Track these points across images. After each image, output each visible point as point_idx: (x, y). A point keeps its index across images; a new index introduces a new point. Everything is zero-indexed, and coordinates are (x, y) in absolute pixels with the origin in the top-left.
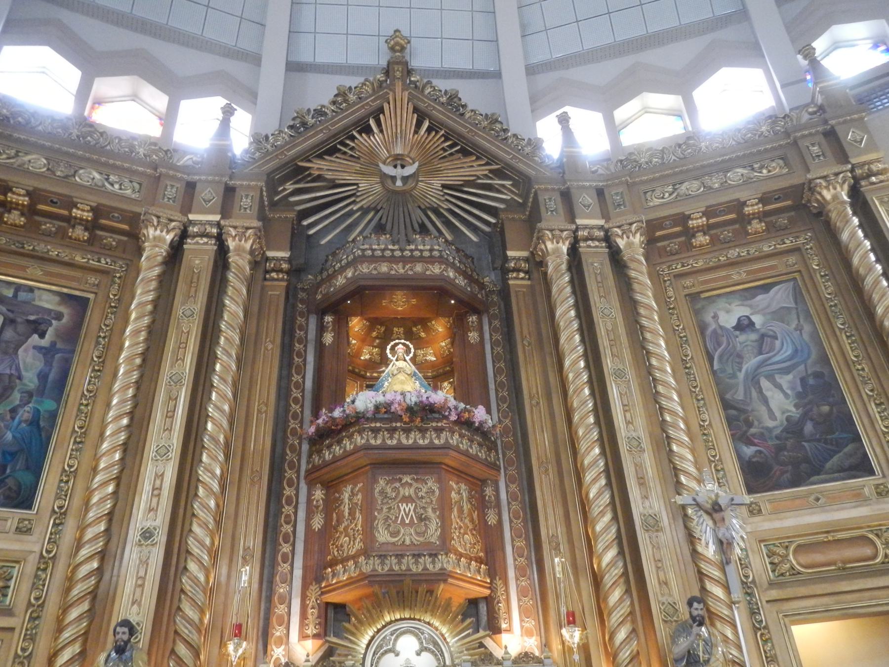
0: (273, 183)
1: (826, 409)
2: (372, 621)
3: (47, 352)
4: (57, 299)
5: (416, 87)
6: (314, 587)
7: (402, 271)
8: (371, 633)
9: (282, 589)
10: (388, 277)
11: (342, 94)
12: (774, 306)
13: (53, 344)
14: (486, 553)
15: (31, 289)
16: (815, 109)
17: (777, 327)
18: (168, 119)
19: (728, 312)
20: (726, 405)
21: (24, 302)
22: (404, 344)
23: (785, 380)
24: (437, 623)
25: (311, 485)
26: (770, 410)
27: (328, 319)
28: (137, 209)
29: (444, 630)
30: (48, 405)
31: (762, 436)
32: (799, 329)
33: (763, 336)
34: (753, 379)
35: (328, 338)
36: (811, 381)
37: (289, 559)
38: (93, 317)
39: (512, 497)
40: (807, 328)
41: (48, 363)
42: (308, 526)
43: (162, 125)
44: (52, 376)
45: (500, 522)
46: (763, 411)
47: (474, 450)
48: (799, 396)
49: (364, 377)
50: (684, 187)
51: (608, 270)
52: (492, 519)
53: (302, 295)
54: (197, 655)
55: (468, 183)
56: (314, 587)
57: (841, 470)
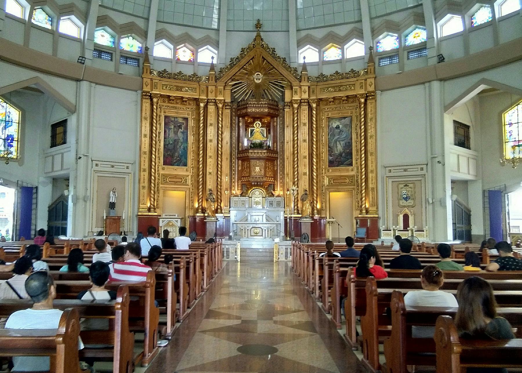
0: (226, 83)
1: (348, 151)
2: (251, 188)
3: (183, 133)
4: (182, 119)
5: (263, 47)
6: (240, 181)
7: (258, 111)
8: (250, 190)
9: (233, 180)
10: (254, 112)
11: (243, 50)
12: (345, 123)
13: (184, 131)
14: (274, 175)
15: (177, 118)
16: (366, 70)
17: (344, 129)
18: (195, 53)
19: (335, 123)
20: (329, 147)
21: (177, 121)
22: (259, 124)
23: (342, 143)
24: (262, 189)
25: (238, 160)
26: (337, 150)
27: (241, 118)
28: (197, 97)
29: (264, 191)
30: (186, 145)
31: (334, 155)
32: (349, 130)
33: (341, 131)
34: (336, 142)
35: (241, 124)
36: (347, 144)
37: (234, 174)
38: (191, 123)
39: (280, 163)
40: (350, 131)
41: (184, 135)
42: (238, 169)
43: (193, 54)
44: (185, 139)
45: (277, 169)
46: (336, 149)
47: (273, 155)
48: (344, 147)
49: (249, 126)
50: (330, 89)
51: (307, 112)
52: (276, 169)
53: (234, 110)
54: (221, 193)
55: (275, 82)
56: (240, 181)
57: (347, 164)
